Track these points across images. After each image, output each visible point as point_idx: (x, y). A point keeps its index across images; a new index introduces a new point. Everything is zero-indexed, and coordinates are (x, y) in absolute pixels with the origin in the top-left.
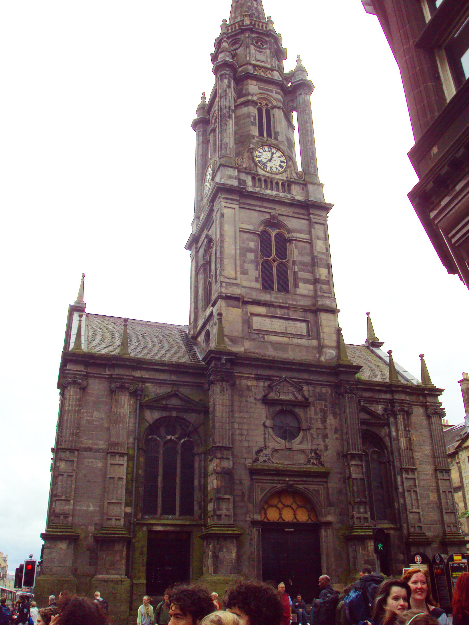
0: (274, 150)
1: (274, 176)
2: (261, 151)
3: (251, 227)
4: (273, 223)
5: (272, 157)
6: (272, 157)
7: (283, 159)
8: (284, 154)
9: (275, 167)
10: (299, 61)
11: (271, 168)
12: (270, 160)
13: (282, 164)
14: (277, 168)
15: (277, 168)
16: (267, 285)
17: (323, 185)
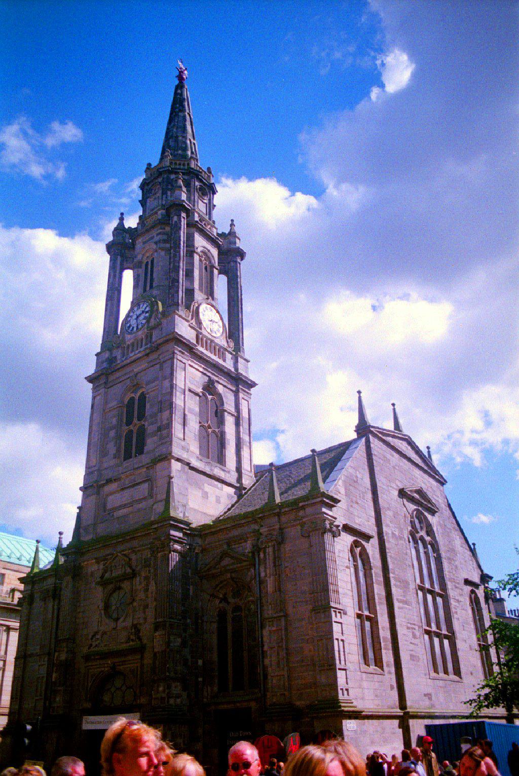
3: (193, 388)
4: (209, 387)
10: (232, 225)
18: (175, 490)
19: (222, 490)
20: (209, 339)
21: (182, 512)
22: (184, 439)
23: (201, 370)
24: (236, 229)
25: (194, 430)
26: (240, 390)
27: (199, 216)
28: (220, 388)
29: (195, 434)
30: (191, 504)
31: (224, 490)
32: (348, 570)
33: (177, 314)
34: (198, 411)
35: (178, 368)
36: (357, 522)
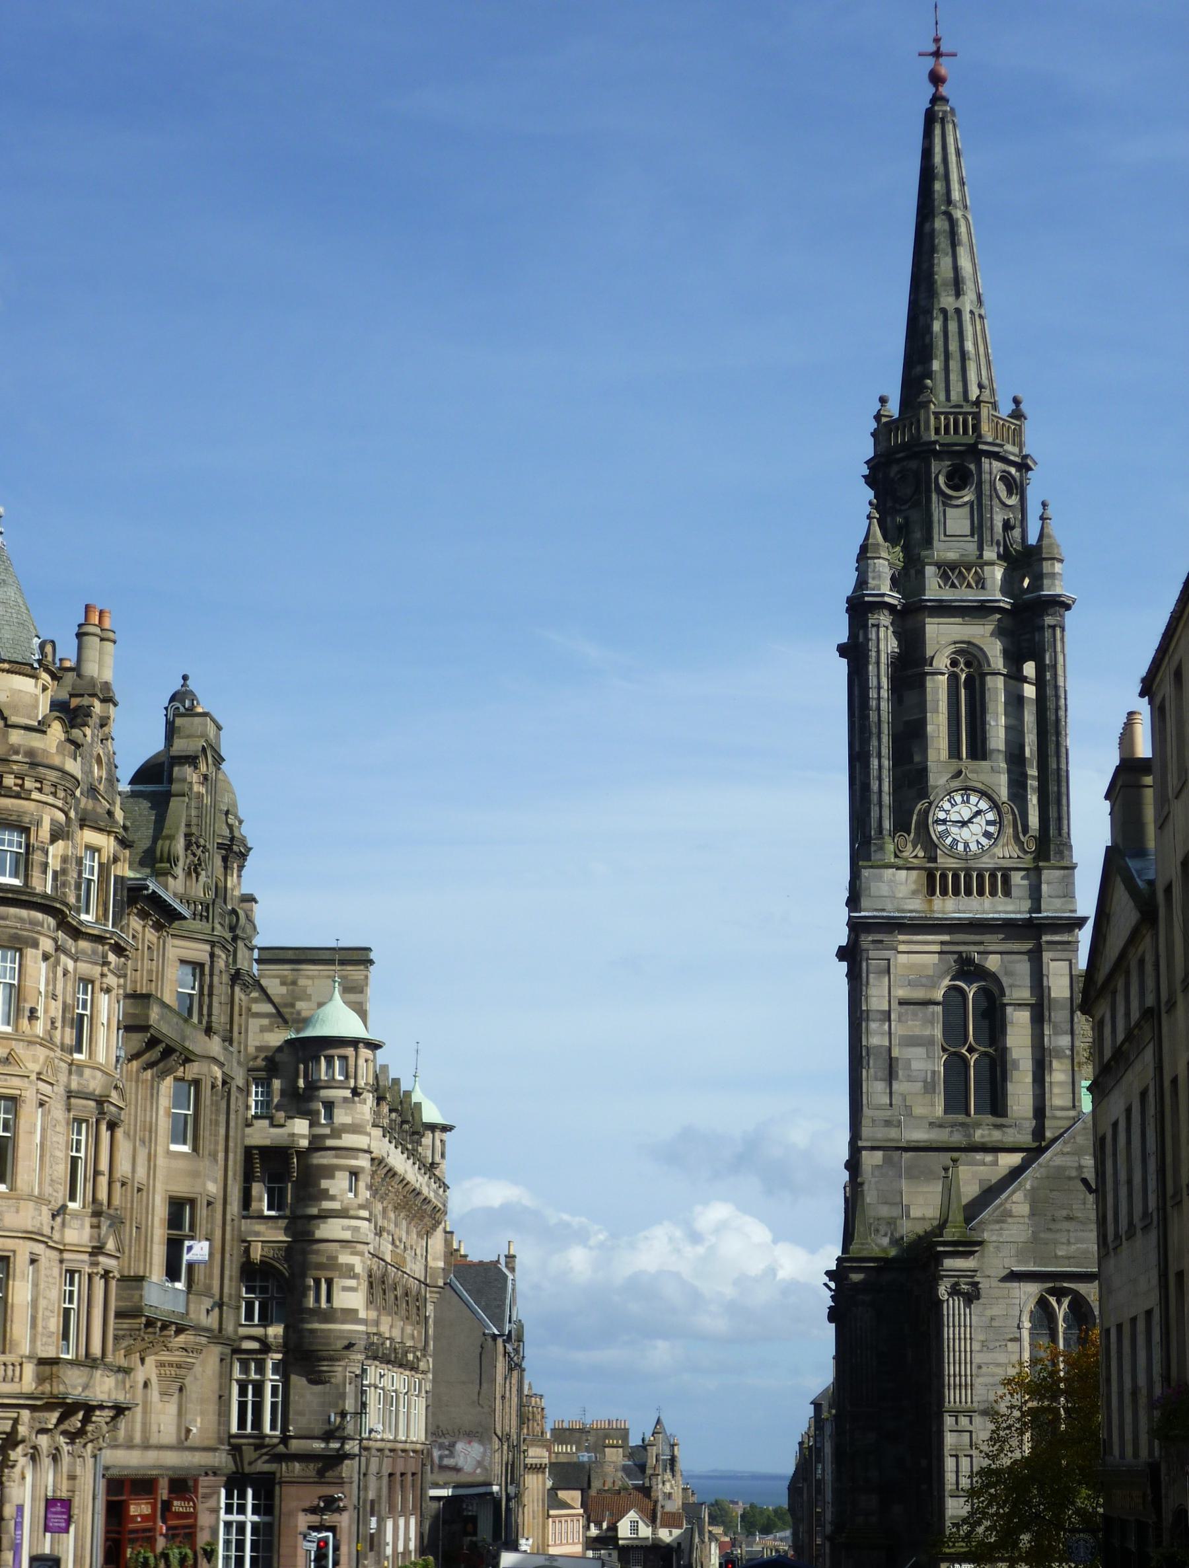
0: (974, 799)
1: (972, 864)
2: (947, 806)
4: (967, 969)
5: (970, 821)
6: (970, 821)
7: (991, 816)
8: (995, 806)
9: (975, 838)
11: (966, 845)
12: (964, 824)
13: (991, 829)
14: (978, 842)
15: (978, 842)
16: (956, 1101)
17: (1073, 868)
18: (868, 1200)
19: (995, 1163)
20: (961, 869)
21: (885, 1235)
22: (891, 1105)
23: (937, 948)
24: (1053, 528)
25: (923, 1075)
26: (1044, 946)
27: (939, 568)
28: (993, 963)
29: (925, 1081)
30: (915, 1212)
31: (1000, 1162)
32: (1013, 1346)
33: (865, 868)
34: (938, 1032)
35: (871, 976)
36: (1060, 1253)
